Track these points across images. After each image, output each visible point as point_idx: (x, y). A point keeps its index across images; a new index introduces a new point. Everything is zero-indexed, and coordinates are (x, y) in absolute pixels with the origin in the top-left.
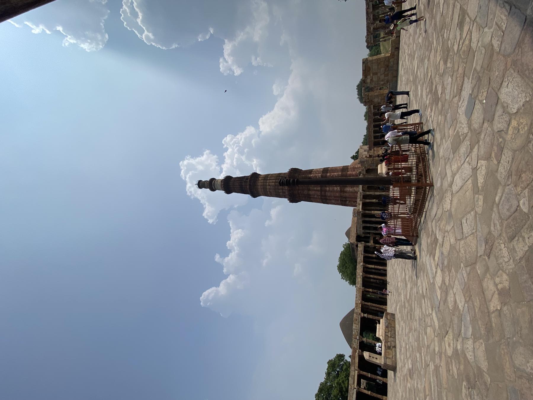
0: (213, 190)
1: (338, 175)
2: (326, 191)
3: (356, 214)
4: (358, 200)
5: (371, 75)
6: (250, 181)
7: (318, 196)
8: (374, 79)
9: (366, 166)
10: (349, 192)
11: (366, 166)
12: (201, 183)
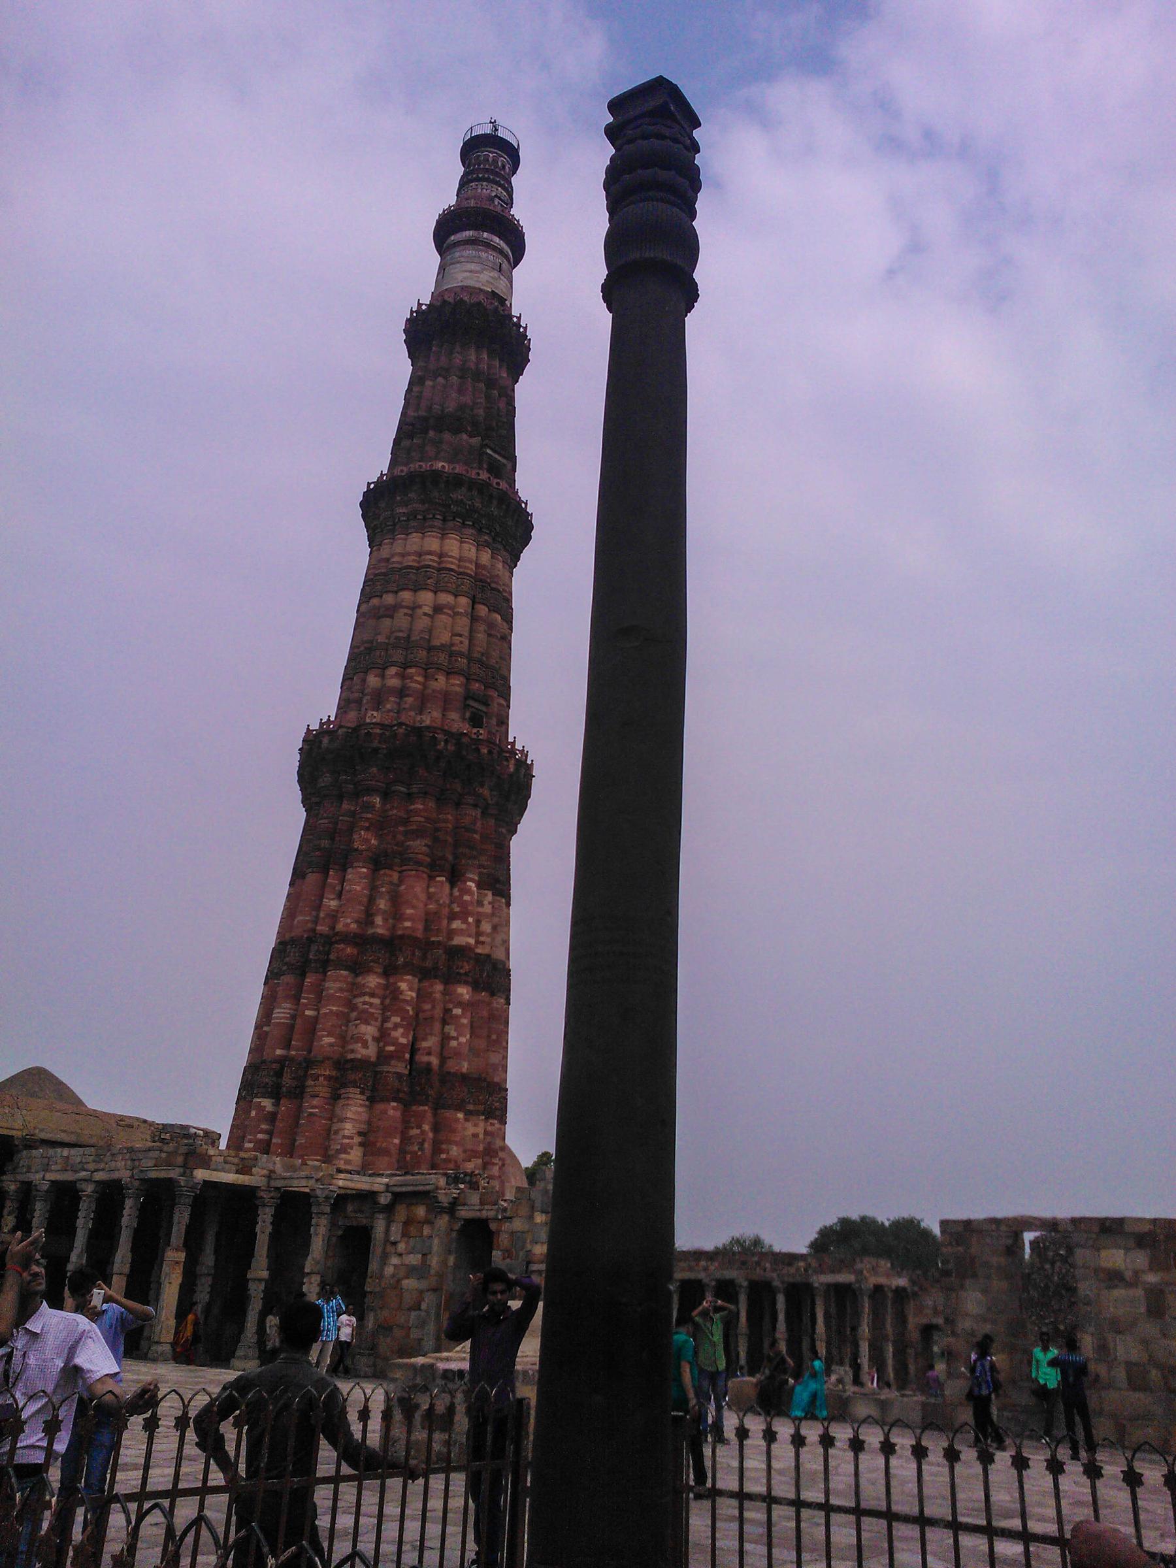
0: (449, 230)
1: (457, 1054)
2: (357, 968)
3: (186, 1144)
4: (277, 1163)
5: (1152, 1278)
6: (482, 488)
7: (334, 916)
8: (1119, 1293)
9: (518, 1225)
11: (518, 1225)
12: (504, 159)
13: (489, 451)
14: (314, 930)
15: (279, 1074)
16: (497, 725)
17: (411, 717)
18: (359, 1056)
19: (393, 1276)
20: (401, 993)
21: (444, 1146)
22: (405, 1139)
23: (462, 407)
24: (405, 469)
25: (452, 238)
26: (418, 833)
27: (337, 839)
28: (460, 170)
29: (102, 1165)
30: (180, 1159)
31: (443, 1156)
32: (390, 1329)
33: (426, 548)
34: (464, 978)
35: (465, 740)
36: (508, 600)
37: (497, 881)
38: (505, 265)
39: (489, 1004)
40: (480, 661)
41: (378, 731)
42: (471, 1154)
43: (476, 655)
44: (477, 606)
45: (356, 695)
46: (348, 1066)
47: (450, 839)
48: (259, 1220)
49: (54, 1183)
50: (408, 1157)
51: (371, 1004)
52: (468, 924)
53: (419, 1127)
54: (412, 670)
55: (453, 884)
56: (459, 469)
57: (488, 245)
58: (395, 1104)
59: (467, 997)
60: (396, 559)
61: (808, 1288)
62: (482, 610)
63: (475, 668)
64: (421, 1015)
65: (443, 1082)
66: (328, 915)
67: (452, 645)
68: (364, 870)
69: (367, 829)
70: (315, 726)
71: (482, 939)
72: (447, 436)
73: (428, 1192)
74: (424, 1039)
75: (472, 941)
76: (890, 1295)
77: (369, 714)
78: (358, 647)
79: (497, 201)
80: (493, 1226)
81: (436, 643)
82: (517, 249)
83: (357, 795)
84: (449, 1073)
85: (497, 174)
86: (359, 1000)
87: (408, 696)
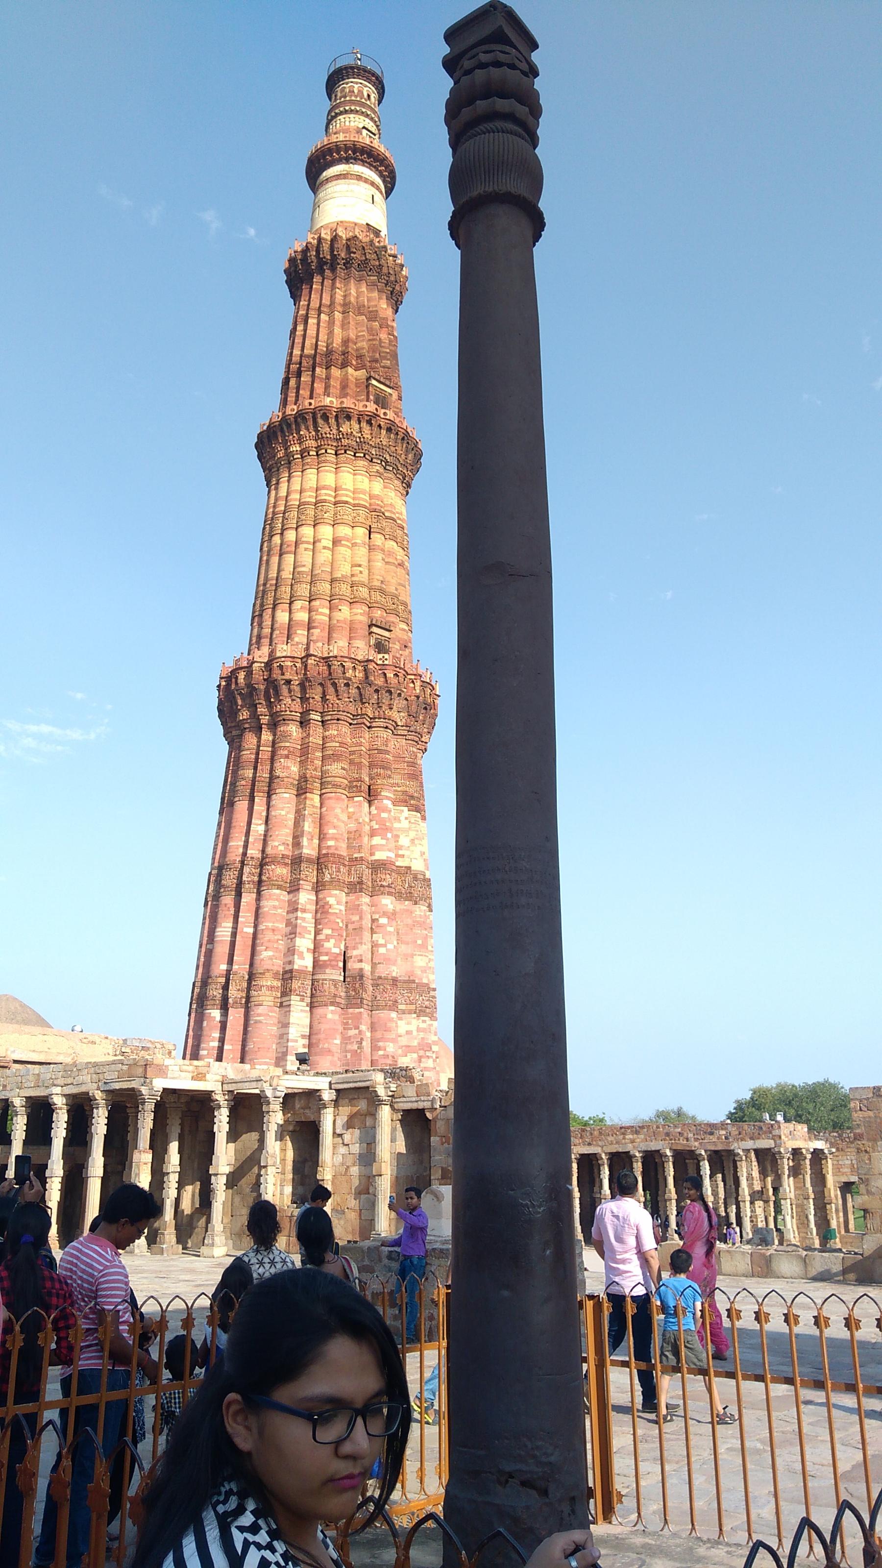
1: (388, 960)
4: (230, 1069)
10: (285, 1025)
12: (368, 89)
14: (244, 854)
15: (226, 987)
17: (319, 649)
18: (296, 967)
19: (343, 1164)
20: (330, 907)
21: (381, 1044)
22: (346, 1040)
23: (346, 342)
24: (295, 407)
25: (324, 174)
26: (336, 757)
27: (259, 767)
29: (69, 1081)
30: (140, 1071)
31: (381, 1053)
32: (343, 1212)
33: (322, 483)
35: (371, 666)
37: (412, 797)
38: (379, 198)
41: (289, 664)
42: (408, 1049)
43: (377, 583)
46: (288, 976)
48: (216, 1120)
49: (28, 1099)
50: (349, 1057)
51: (304, 919)
52: (388, 839)
53: (357, 1028)
54: (316, 603)
56: (348, 403)
57: (359, 178)
58: (332, 1008)
59: (391, 907)
61: (731, 1154)
62: (378, 539)
63: (377, 596)
64: (350, 927)
65: (375, 986)
66: (255, 839)
67: (352, 575)
69: (287, 757)
71: (400, 852)
72: (336, 372)
73: (368, 1087)
74: (355, 948)
75: (392, 855)
76: (809, 1156)
77: (278, 649)
80: (429, 1115)
81: (338, 575)
83: (274, 726)
84: (380, 978)
85: (363, 105)
86: (291, 916)
87: (314, 628)
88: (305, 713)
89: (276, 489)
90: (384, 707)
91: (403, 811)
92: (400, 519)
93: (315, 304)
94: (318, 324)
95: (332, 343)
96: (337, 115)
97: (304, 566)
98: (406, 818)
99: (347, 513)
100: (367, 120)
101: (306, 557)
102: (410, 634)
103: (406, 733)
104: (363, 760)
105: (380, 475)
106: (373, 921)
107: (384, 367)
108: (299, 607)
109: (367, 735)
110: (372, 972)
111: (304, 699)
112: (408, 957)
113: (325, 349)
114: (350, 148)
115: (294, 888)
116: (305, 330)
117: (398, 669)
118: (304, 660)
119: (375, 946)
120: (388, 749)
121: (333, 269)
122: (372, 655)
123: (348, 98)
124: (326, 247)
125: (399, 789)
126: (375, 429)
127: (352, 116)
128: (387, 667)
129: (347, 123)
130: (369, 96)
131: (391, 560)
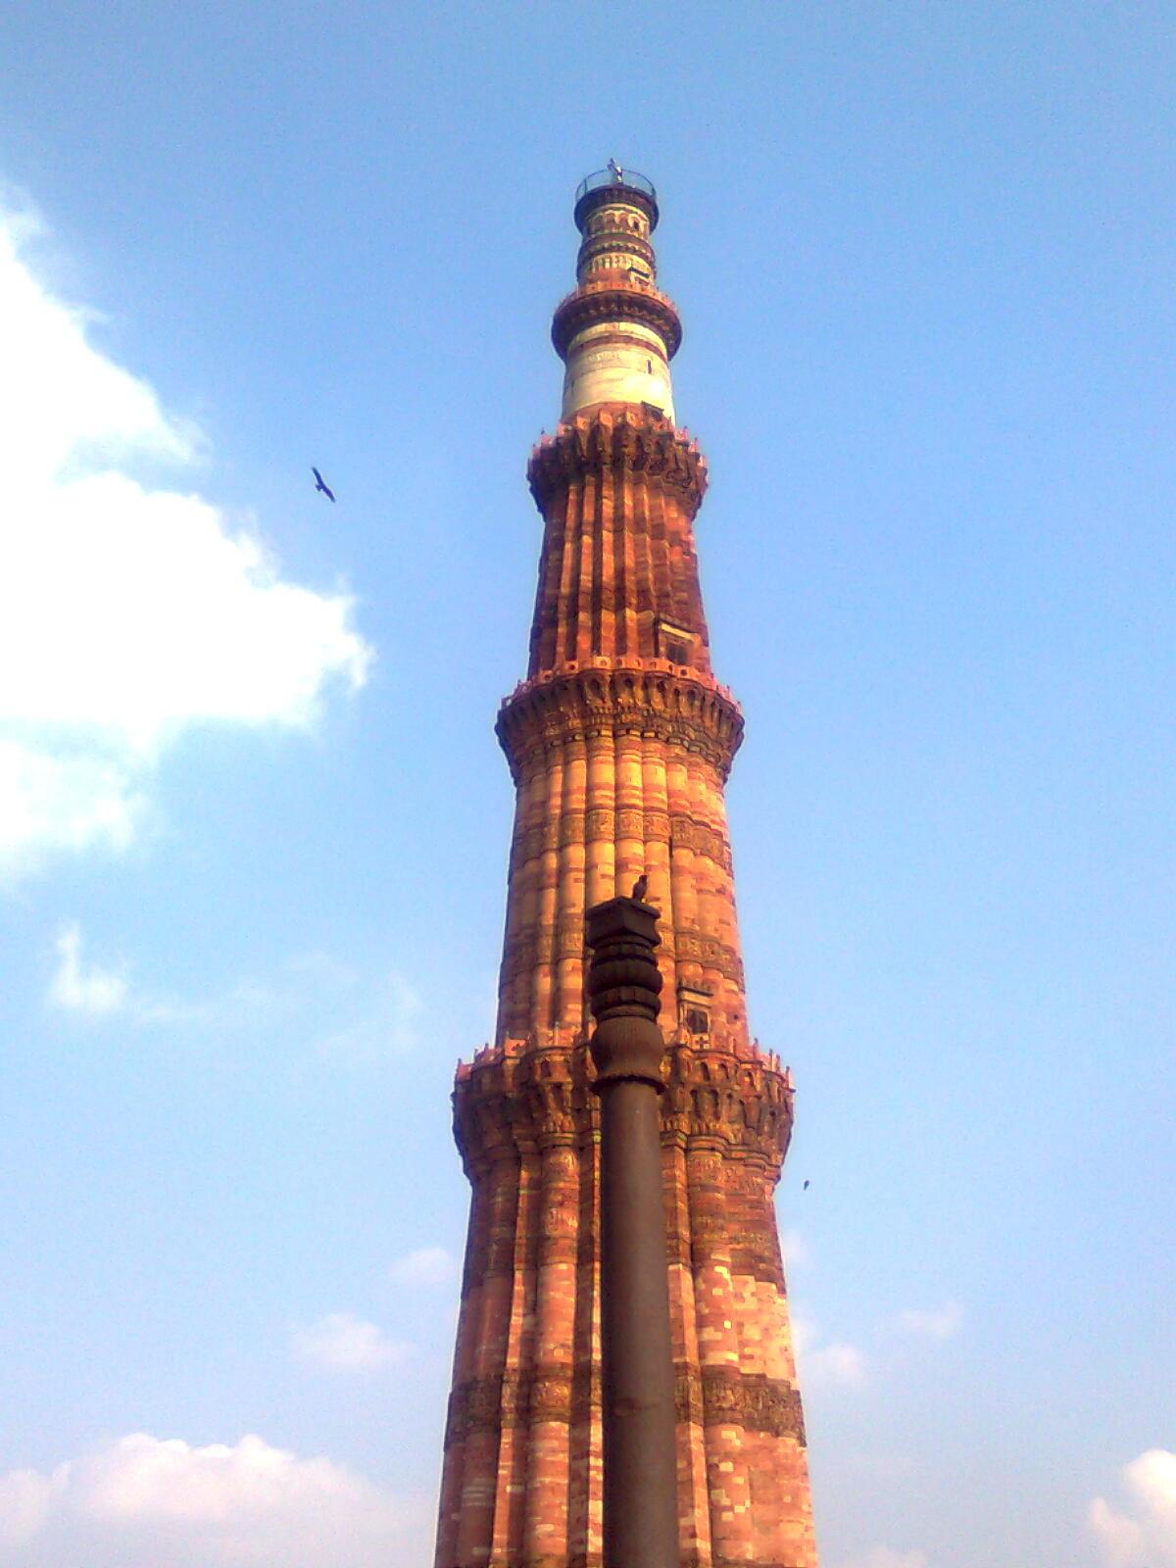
0: (574, 327)
1: (737, 1534)
6: (662, 683)
12: (636, 215)
13: (665, 627)
14: (505, 1363)
16: (728, 1022)
23: (620, 573)
24: (550, 672)
25: (578, 338)
28: (576, 239)
34: (729, 1414)
35: (685, 1054)
36: (720, 835)
37: (761, 1259)
39: (772, 1450)
40: (692, 934)
43: (685, 924)
44: (674, 853)
45: (522, 1006)
47: (682, 1206)
51: (596, 1468)
52: (725, 1331)
55: (695, 1273)
57: (629, 340)
60: (557, 801)
62: (685, 857)
68: (563, 1267)
69: (561, 1204)
70: (469, 1060)
71: (748, 1351)
74: (685, 1515)
75: (733, 1357)
78: (517, 935)
79: (633, 275)
82: (672, 333)
85: (630, 238)
86: (581, 1464)
88: (585, 1132)
89: (528, 791)
90: (708, 1118)
91: (745, 1283)
92: (713, 822)
93: (571, 523)
94: (578, 551)
95: (601, 575)
96: (592, 255)
97: (574, 905)
98: (753, 1294)
99: (636, 821)
100: (635, 258)
101: (577, 894)
102: (741, 995)
103: (744, 1155)
104: (680, 1204)
105: (679, 760)
106: (711, 1467)
107: (678, 602)
108: (570, 969)
109: (681, 1163)
110: (713, 1553)
111: (580, 1112)
112: (769, 1526)
113: (590, 585)
114: (613, 301)
115: (579, 1418)
116: (561, 560)
117: (725, 1057)
118: (581, 1050)
119: (715, 1510)
120: (719, 1184)
121: (599, 473)
122: (685, 1036)
123: (607, 231)
124: (584, 441)
125: (741, 1246)
126: (671, 697)
127: (613, 255)
128: (710, 1055)
129: (607, 265)
130: (636, 225)
131: (706, 886)
